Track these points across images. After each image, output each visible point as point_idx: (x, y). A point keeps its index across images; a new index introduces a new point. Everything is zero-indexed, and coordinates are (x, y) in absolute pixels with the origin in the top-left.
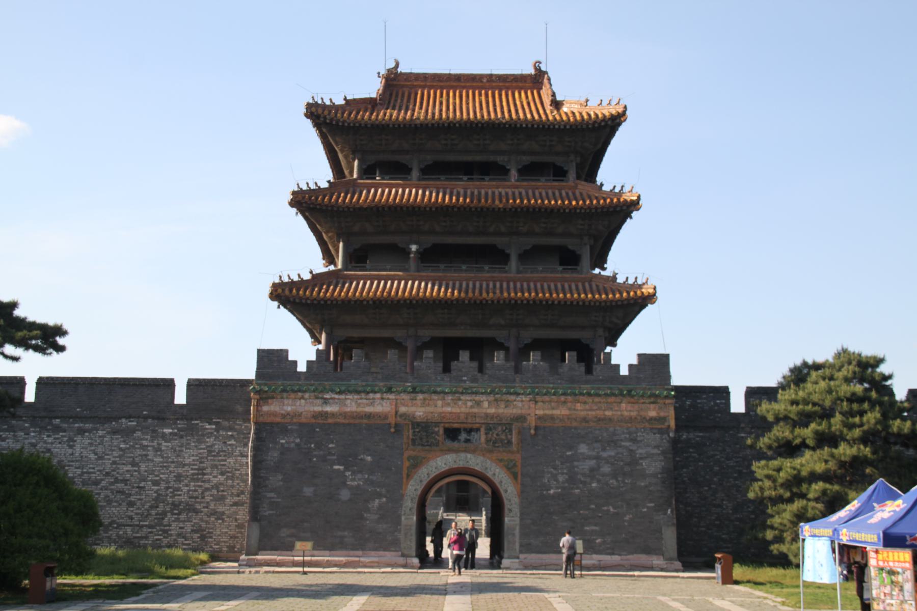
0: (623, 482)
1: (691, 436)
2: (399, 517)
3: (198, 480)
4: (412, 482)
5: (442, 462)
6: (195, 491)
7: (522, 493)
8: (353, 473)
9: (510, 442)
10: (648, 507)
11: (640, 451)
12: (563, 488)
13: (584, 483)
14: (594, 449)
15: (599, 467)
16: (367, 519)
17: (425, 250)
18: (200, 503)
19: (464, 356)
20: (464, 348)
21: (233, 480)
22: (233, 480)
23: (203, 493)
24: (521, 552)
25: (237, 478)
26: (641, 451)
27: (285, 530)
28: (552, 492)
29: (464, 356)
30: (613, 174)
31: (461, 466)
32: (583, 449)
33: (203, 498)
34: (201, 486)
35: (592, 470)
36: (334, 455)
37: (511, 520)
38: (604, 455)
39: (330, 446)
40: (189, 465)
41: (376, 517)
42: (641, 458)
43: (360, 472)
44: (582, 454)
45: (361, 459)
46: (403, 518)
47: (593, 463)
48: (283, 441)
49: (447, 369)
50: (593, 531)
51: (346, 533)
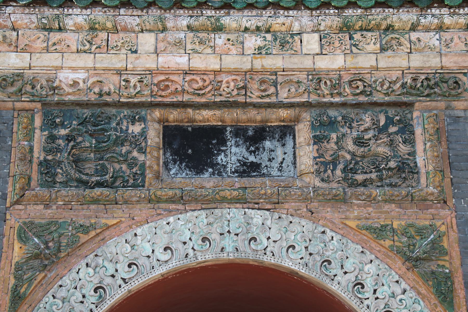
9: (407, 169)
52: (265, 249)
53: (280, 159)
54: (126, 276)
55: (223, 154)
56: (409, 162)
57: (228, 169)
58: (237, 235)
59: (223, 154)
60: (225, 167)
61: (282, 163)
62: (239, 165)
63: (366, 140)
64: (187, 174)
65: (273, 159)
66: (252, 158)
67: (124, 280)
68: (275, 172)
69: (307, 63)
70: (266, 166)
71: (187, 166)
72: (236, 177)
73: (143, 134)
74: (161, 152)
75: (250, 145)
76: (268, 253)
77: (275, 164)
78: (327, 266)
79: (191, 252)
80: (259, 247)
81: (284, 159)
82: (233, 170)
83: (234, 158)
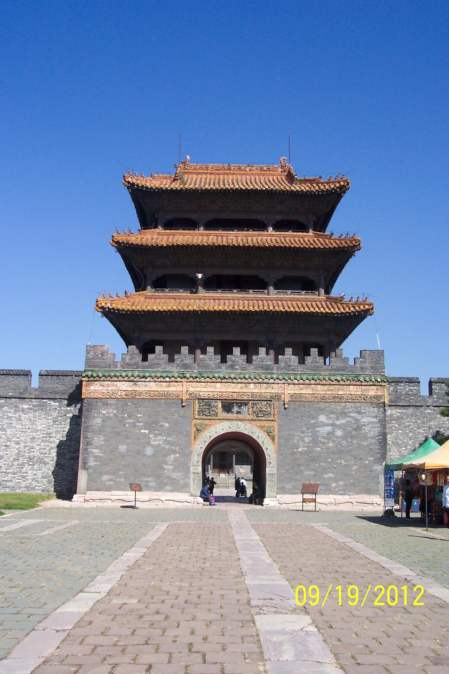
0: (351, 442)
1: (394, 412)
2: (189, 467)
3: (46, 441)
4: (198, 442)
6: (44, 449)
7: (279, 451)
8: (155, 435)
10: (369, 460)
11: (363, 420)
12: (308, 447)
13: (323, 443)
14: (330, 419)
15: (334, 431)
16: (164, 469)
17: (208, 279)
18: (49, 457)
19: (237, 351)
20: (236, 346)
21: (71, 442)
22: (71, 442)
23: (49, 451)
24: (278, 493)
25: (74, 440)
26: (365, 420)
27: (106, 476)
28: (300, 450)
29: (237, 351)
30: (340, 226)
32: (322, 418)
33: (50, 454)
34: (48, 446)
35: (329, 434)
36: (141, 422)
37: (271, 470)
38: (338, 423)
39: (139, 416)
40: (41, 430)
41: (171, 467)
42: (364, 425)
43: (160, 435)
44: (322, 422)
45: (161, 426)
46: (191, 469)
47: (329, 428)
48: (105, 412)
49: (224, 360)
50: (330, 477)
51: (150, 479)
69: (251, 391)
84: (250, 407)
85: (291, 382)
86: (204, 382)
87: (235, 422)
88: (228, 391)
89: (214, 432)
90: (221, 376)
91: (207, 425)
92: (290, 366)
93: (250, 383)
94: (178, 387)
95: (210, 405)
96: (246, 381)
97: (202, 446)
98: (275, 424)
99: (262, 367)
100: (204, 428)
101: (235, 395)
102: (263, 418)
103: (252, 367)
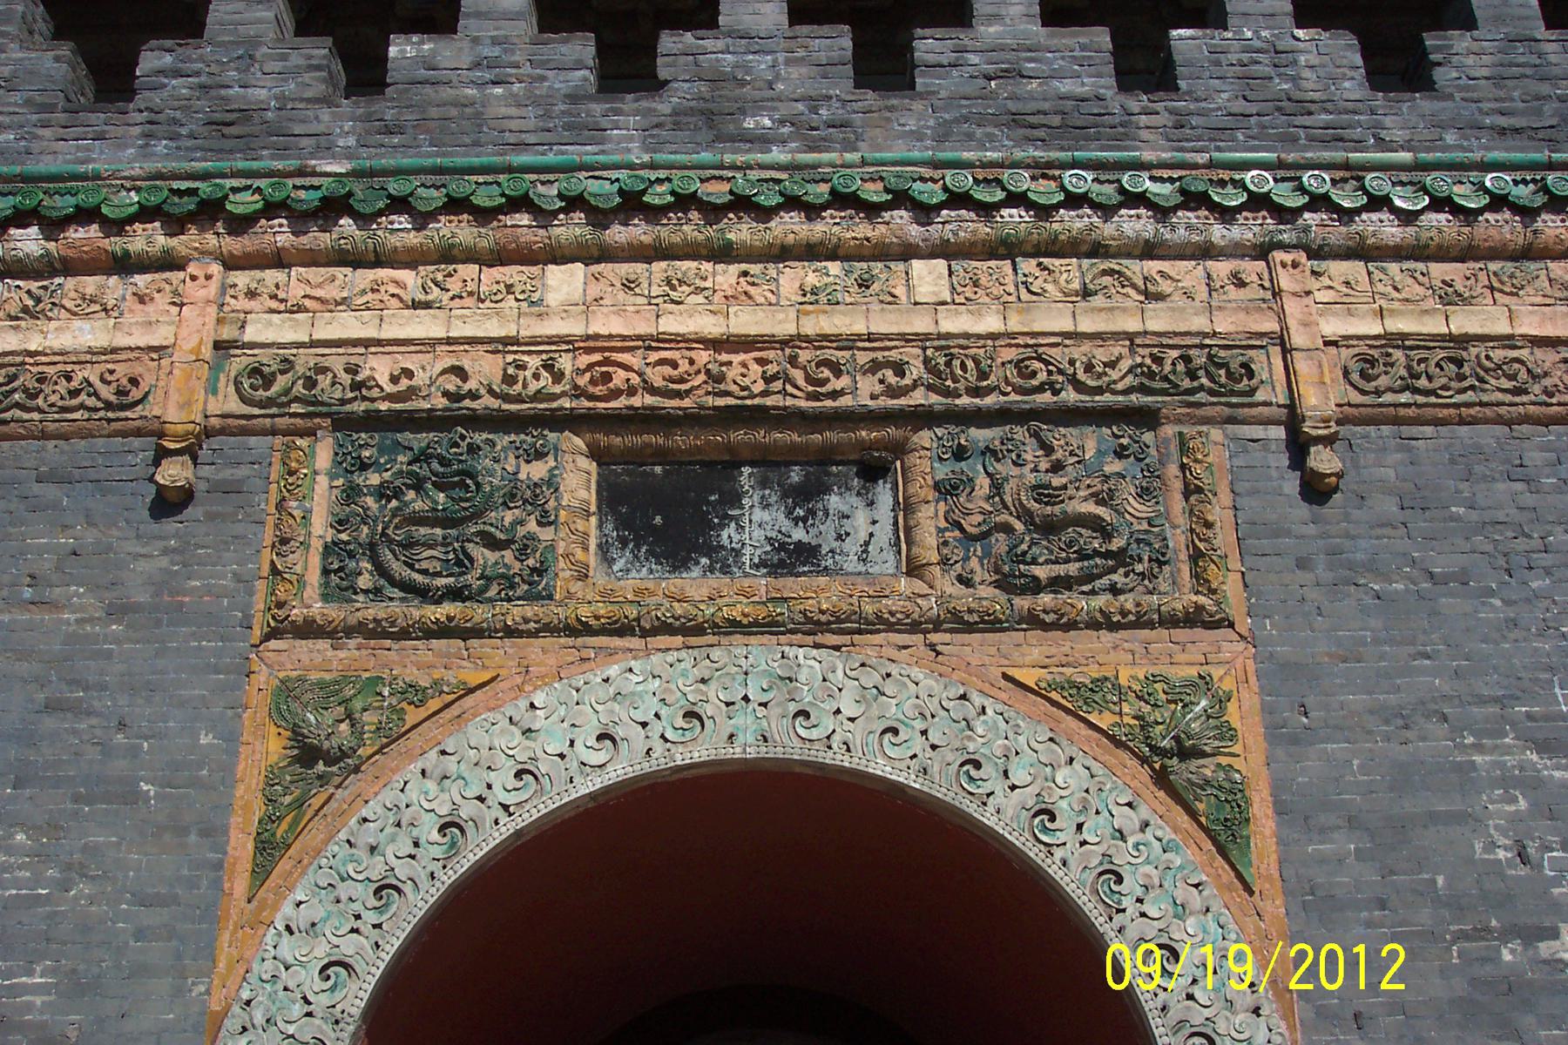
4: (300, 899)
5: (572, 723)
31: (747, 748)
52: (828, 737)
53: (863, 536)
54: (509, 799)
55: (733, 525)
56: (1151, 538)
57: (746, 559)
58: (764, 705)
59: (733, 525)
60: (737, 553)
61: (867, 544)
62: (769, 548)
63: (1055, 489)
64: (651, 571)
65: (848, 534)
66: (799, 534)
67: (506, 807)
68: (851, 564)
69: (921, 324)
70: (832, 551)
71: (650, 553)
72: (764, 576)
73: (551, 482)
74: (594, 520)
75: (796, 505)
76: (835, 746)
77: (852, 547)
78: (973, 773)
79: (659, 748)
80: (814, 734)
81: (871, 535)
82: (756, 560)
83: (758, 534)
84: (921, 488)
85: (1337, 234)
86: (411, 259)
87: (761, 654)
88: (671, 324)
89: (503, 778)
90: (600, 189)
91: (414, 694)
92: (1304, 107)
93: (908, 252)
94: (135, 314)
95: (459, 479)
96: (861, 230)
97: (349, 947)
98: (1228, 660)
99: (1015, 120)
100: (391, 738)
101: (745, 373)
102: (1082, 603)
103: (913, 115)
